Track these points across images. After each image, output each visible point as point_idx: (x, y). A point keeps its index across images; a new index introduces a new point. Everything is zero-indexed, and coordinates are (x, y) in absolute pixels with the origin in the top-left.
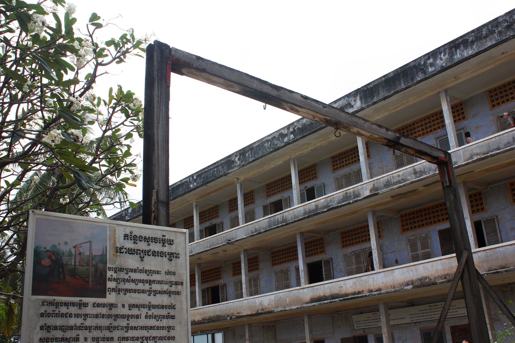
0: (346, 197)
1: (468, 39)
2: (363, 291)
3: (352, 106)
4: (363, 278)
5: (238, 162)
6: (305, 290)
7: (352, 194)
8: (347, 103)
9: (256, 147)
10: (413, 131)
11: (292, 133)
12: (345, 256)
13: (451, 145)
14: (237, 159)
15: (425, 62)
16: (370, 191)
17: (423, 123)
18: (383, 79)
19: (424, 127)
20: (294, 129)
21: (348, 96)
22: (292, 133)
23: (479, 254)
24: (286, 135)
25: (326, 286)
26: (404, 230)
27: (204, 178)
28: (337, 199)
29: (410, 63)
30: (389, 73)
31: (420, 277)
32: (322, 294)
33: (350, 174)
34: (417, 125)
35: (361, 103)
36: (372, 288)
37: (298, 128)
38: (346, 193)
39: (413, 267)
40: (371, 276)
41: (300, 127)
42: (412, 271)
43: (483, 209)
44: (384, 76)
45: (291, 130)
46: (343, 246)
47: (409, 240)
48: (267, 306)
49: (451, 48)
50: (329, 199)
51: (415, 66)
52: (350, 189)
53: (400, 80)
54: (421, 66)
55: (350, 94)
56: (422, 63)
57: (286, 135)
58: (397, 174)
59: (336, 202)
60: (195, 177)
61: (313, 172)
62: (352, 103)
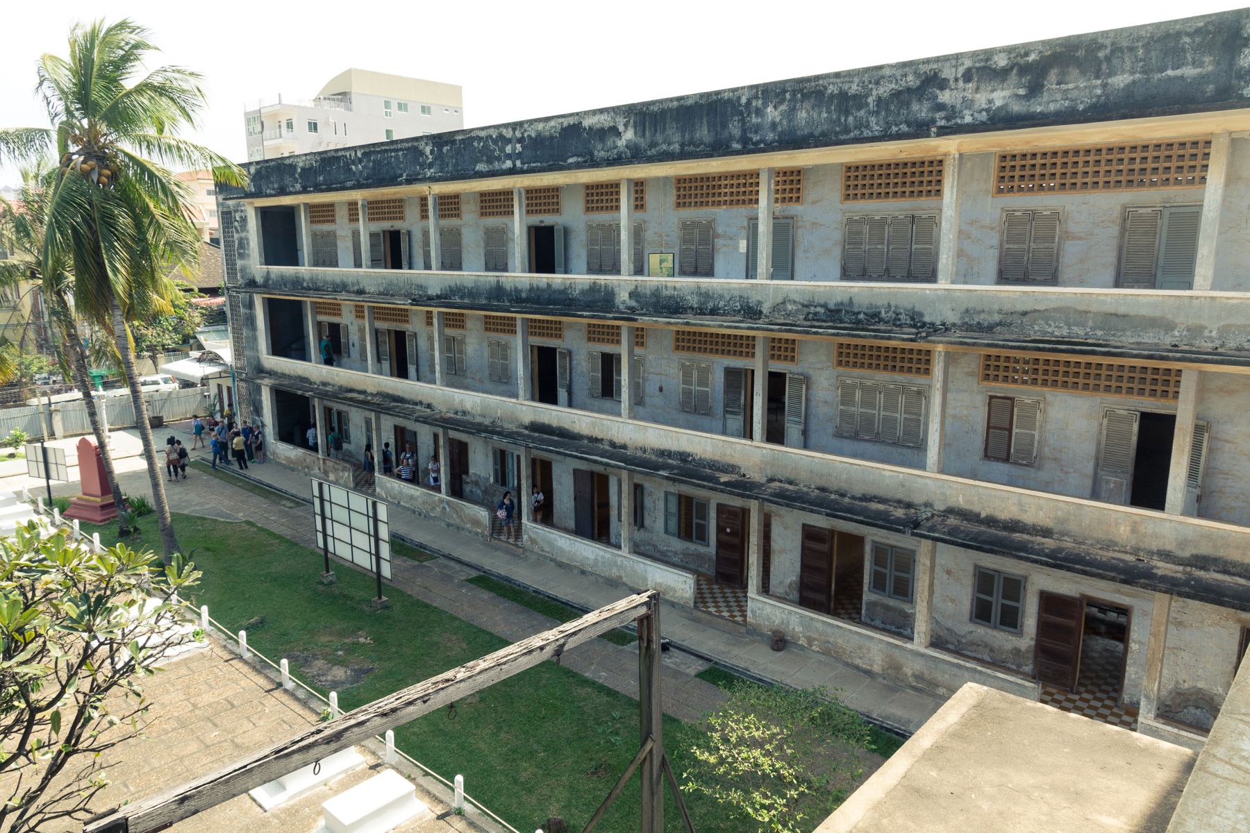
0: (594, 288)
1: (825, 88)
2: (602, 439)
3: (619, 134)
4: (605, 422)
5: (430, 157)
6: (524, 408)
7: (603, 288)
8: (612, 124)
9: (460, 140)
10: (717, 191)
11: (520, 141)
12: (590, 354)
13: (759, 270)
14: (428, 150)
15: (749, 102)
16: (630, 294)
17: (735, 182)
18: (675, 103)
19: (734, 190)
20: (523, 134)
21: (615, 110)
22: (520, 141)
23: (764, 451)
24: (509, 141)
25: (554, 413)
26: (677, 348)
27: (374, 162)
28: (580, 287)
29: (725, 91)
30: (688, 97)
31: (681, 449)
32: (547, 422)
33: (610, 225)
34: (723, 182)
35: (635, 133)
36: (616, 440)
37: (529, 136)
38: (595, 283)
39: (674, 434)
40: (617, 424)
41: (533, 135)
42: (671, 438)
43: (793, 359)
44: (679, 99)
45: (518, 134)
46: (589, 339)
47: (683, 365)
48: (470, 409)
49: (794, 93)
50: (569, 282)
51: (729, 101)
52: (602, 279)
53: (702, 119)
54: (740, 105)
55: (618, 107)
56: (744, 100)
57: (509, 141)
58: (673, 284)
59: (577, 292)
60: (359, 154)
61: (555, 200)
62: (621, 128)
